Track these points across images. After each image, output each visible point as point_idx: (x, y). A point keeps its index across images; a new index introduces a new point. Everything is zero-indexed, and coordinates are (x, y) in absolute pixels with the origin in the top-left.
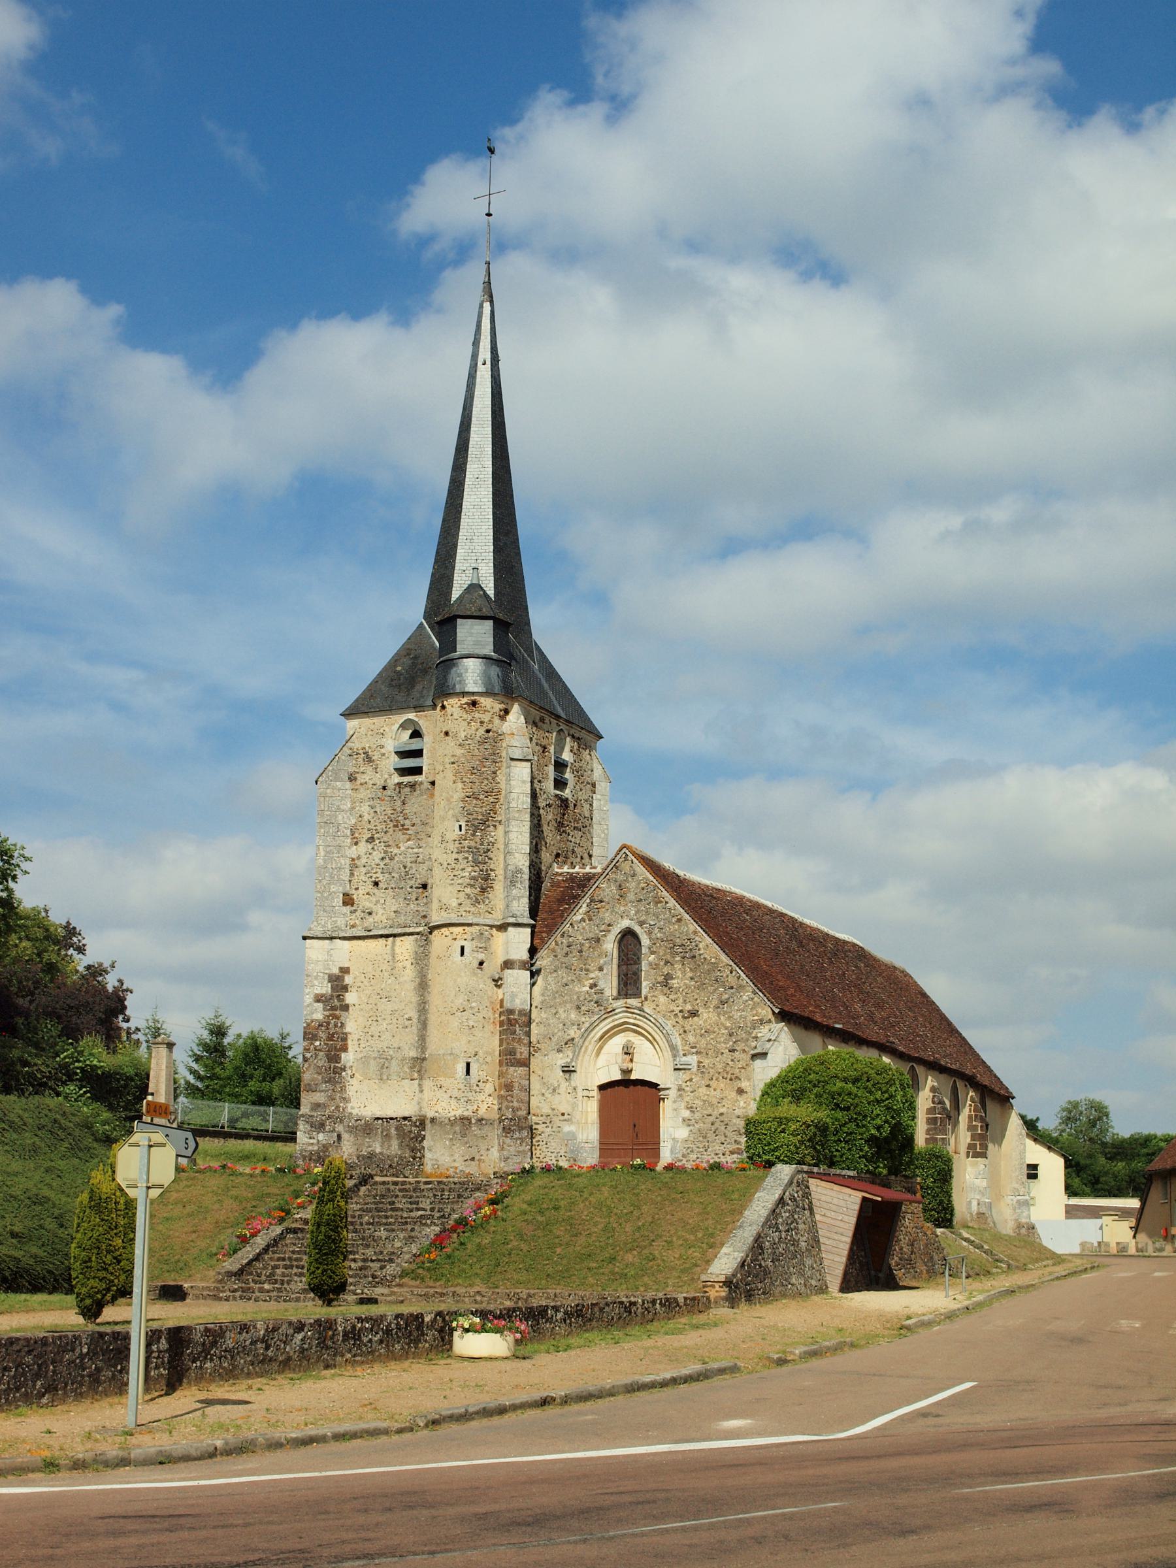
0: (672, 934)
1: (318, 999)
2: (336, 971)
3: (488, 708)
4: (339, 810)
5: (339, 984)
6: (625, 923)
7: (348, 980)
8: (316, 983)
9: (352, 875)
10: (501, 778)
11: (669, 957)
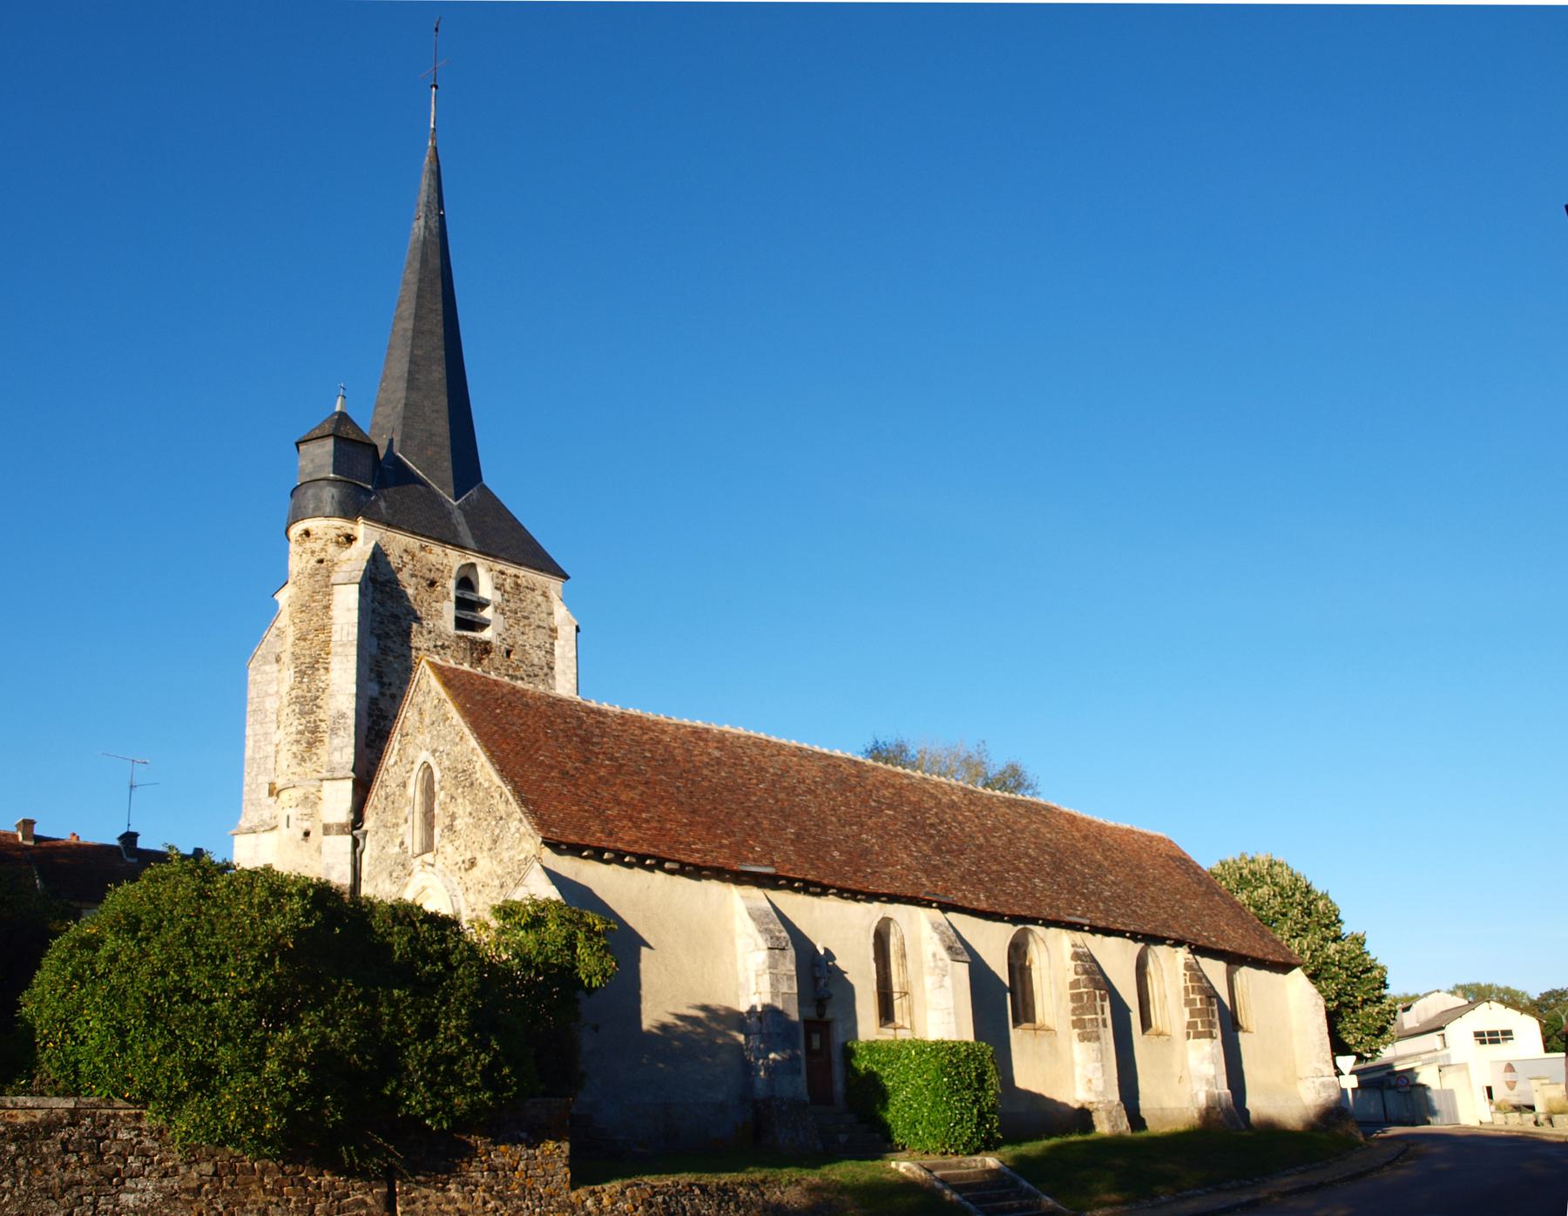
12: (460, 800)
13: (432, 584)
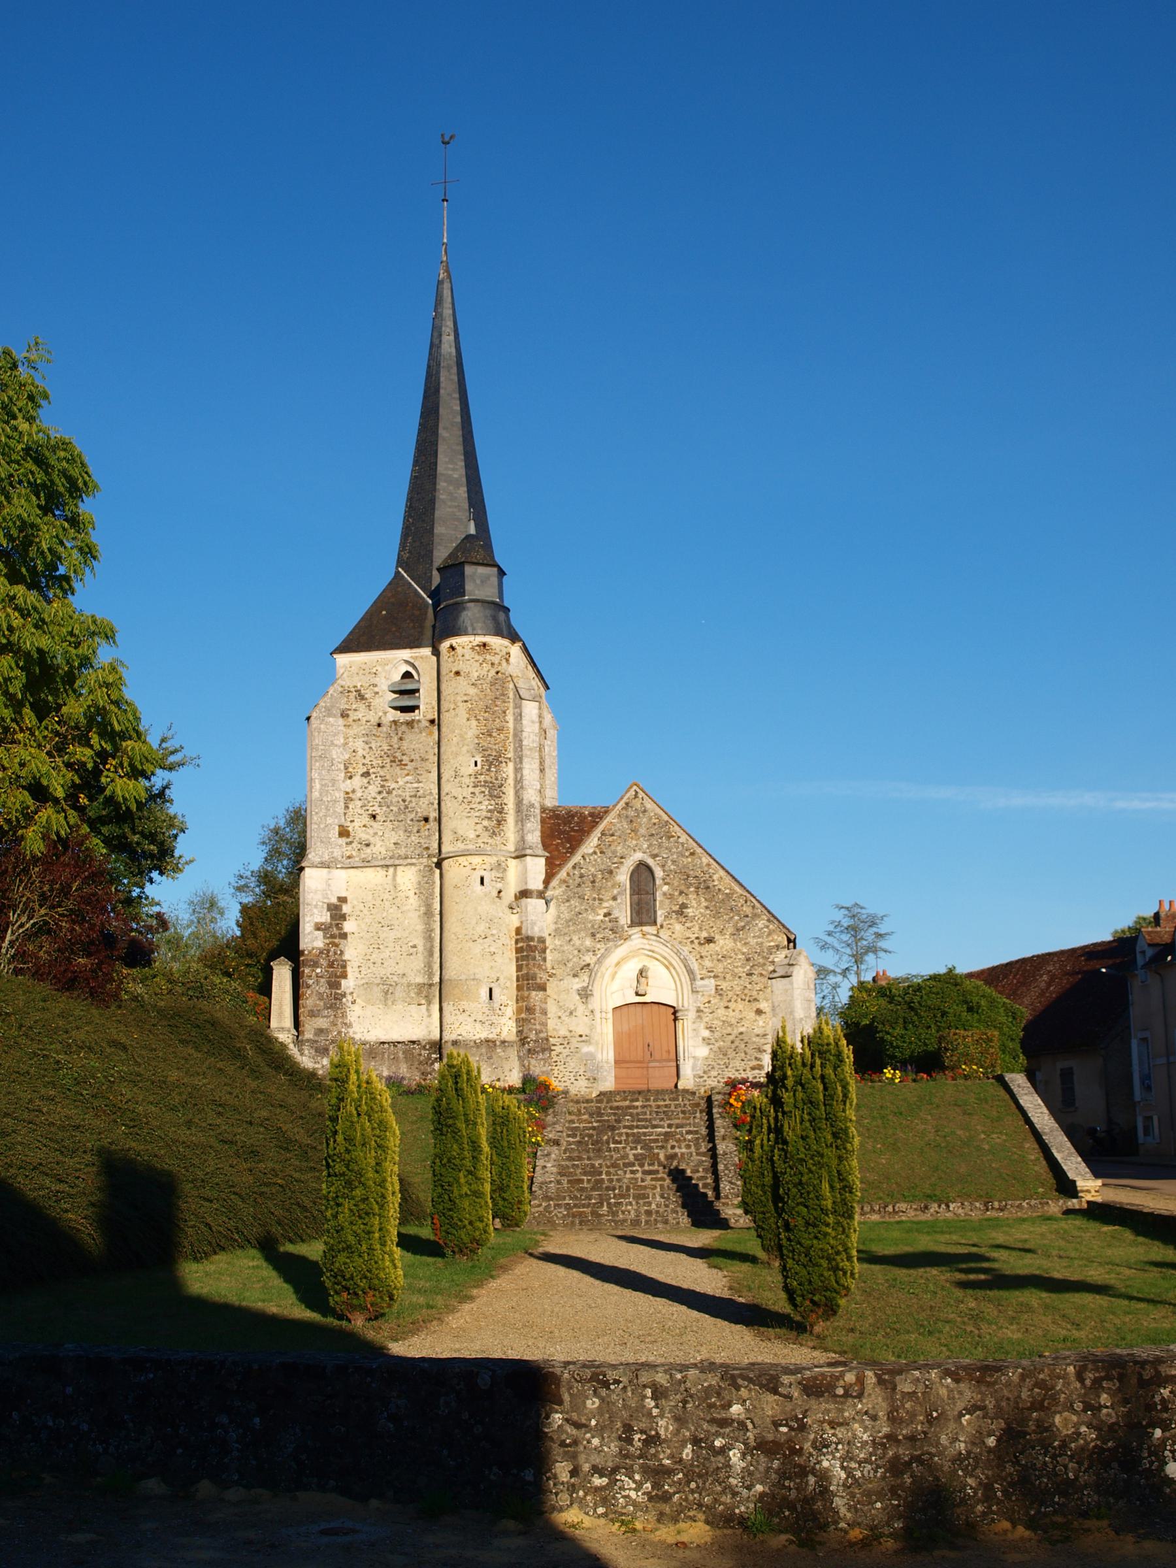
0: (684, 866)
1: (318, 927)
2: (334, 900)
4: (332, 743)
5: (337, 912)
6: (639, 856)
7: (346, 909)
8: (315, 911)
9: (347, 807)
10: (510, 718)
11: (683, 888)
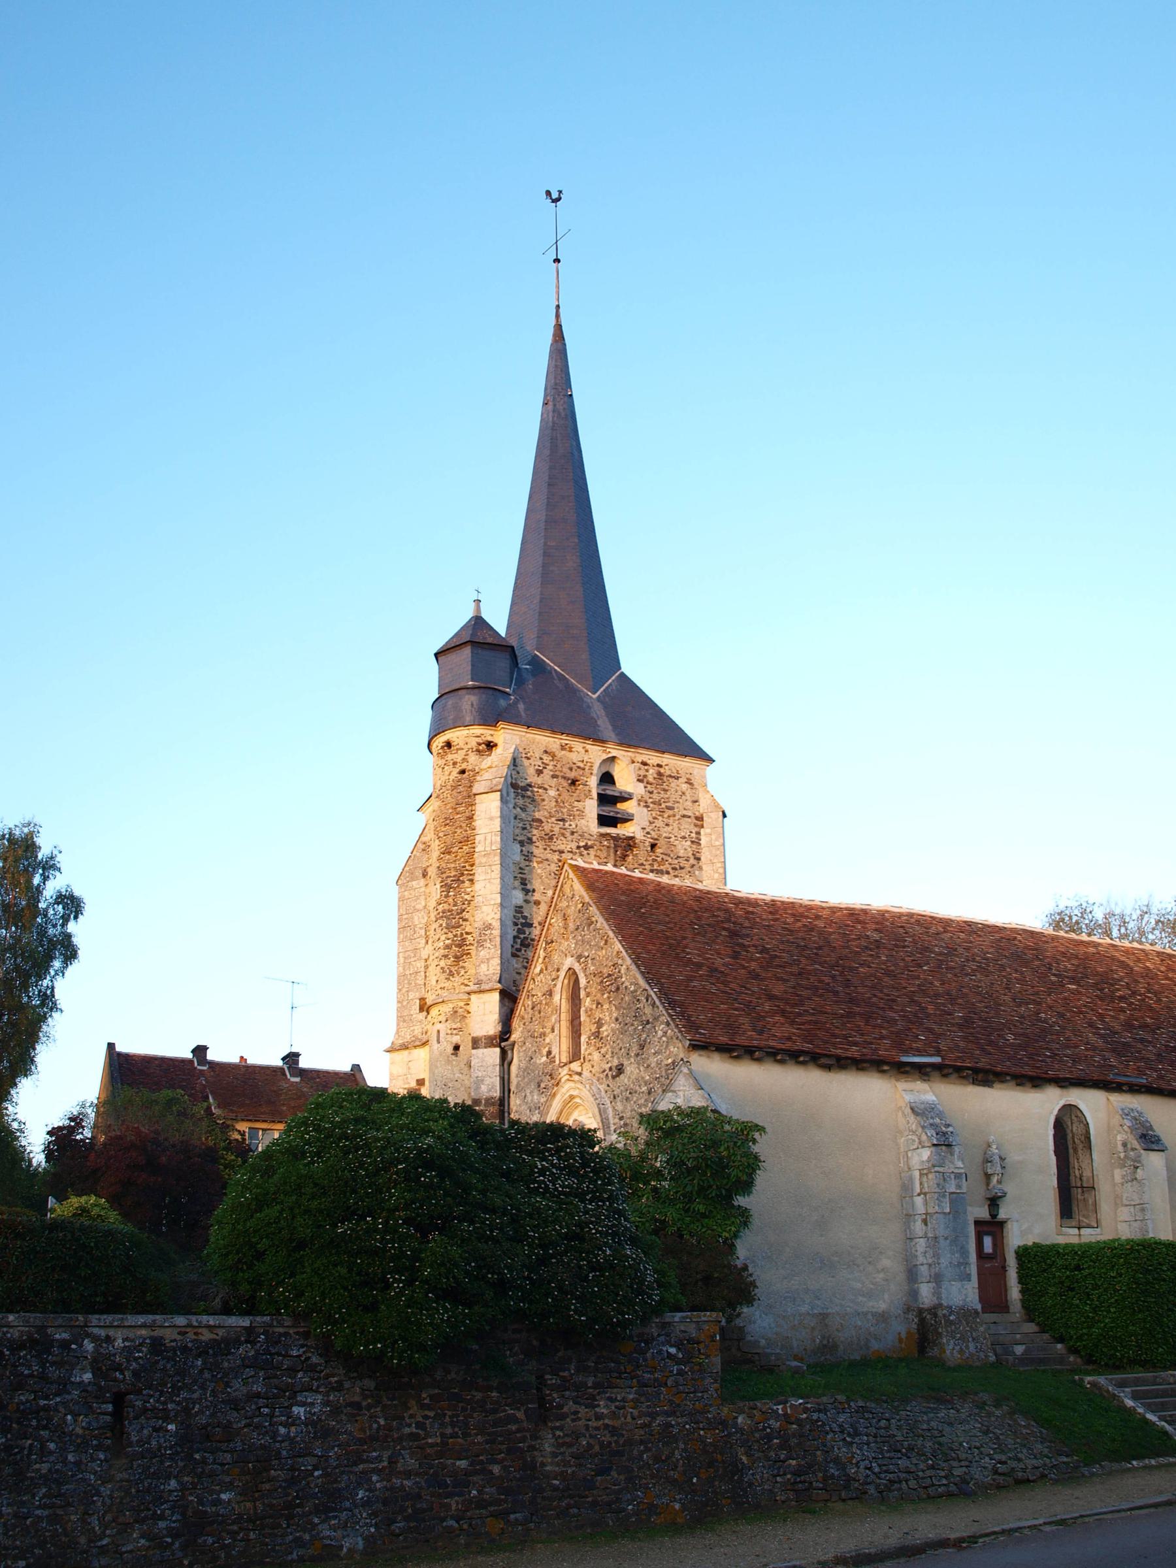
3: (461, 745)
12: (606, 1006)
13: (574, 782)
